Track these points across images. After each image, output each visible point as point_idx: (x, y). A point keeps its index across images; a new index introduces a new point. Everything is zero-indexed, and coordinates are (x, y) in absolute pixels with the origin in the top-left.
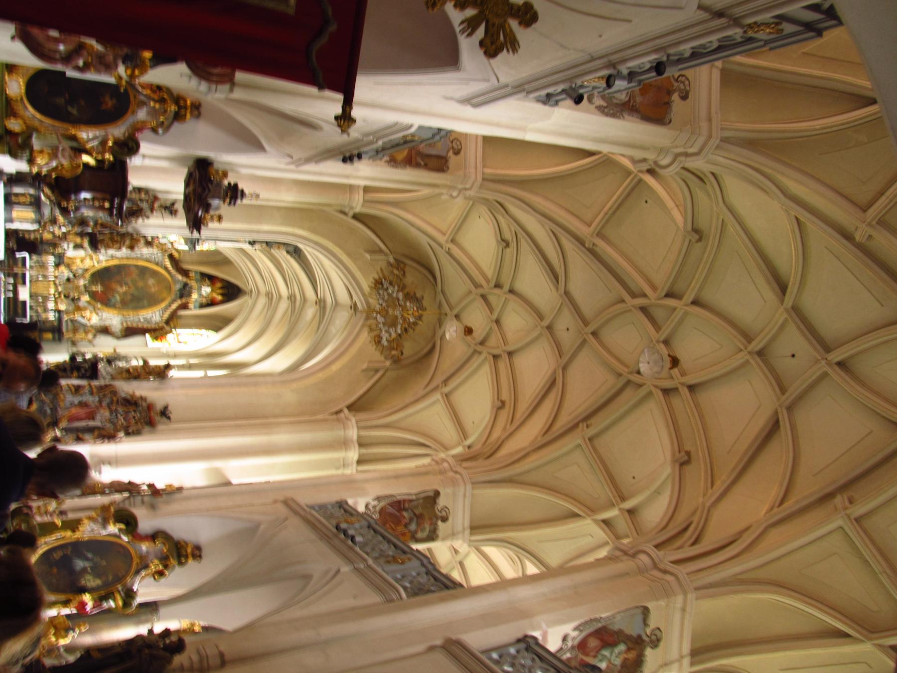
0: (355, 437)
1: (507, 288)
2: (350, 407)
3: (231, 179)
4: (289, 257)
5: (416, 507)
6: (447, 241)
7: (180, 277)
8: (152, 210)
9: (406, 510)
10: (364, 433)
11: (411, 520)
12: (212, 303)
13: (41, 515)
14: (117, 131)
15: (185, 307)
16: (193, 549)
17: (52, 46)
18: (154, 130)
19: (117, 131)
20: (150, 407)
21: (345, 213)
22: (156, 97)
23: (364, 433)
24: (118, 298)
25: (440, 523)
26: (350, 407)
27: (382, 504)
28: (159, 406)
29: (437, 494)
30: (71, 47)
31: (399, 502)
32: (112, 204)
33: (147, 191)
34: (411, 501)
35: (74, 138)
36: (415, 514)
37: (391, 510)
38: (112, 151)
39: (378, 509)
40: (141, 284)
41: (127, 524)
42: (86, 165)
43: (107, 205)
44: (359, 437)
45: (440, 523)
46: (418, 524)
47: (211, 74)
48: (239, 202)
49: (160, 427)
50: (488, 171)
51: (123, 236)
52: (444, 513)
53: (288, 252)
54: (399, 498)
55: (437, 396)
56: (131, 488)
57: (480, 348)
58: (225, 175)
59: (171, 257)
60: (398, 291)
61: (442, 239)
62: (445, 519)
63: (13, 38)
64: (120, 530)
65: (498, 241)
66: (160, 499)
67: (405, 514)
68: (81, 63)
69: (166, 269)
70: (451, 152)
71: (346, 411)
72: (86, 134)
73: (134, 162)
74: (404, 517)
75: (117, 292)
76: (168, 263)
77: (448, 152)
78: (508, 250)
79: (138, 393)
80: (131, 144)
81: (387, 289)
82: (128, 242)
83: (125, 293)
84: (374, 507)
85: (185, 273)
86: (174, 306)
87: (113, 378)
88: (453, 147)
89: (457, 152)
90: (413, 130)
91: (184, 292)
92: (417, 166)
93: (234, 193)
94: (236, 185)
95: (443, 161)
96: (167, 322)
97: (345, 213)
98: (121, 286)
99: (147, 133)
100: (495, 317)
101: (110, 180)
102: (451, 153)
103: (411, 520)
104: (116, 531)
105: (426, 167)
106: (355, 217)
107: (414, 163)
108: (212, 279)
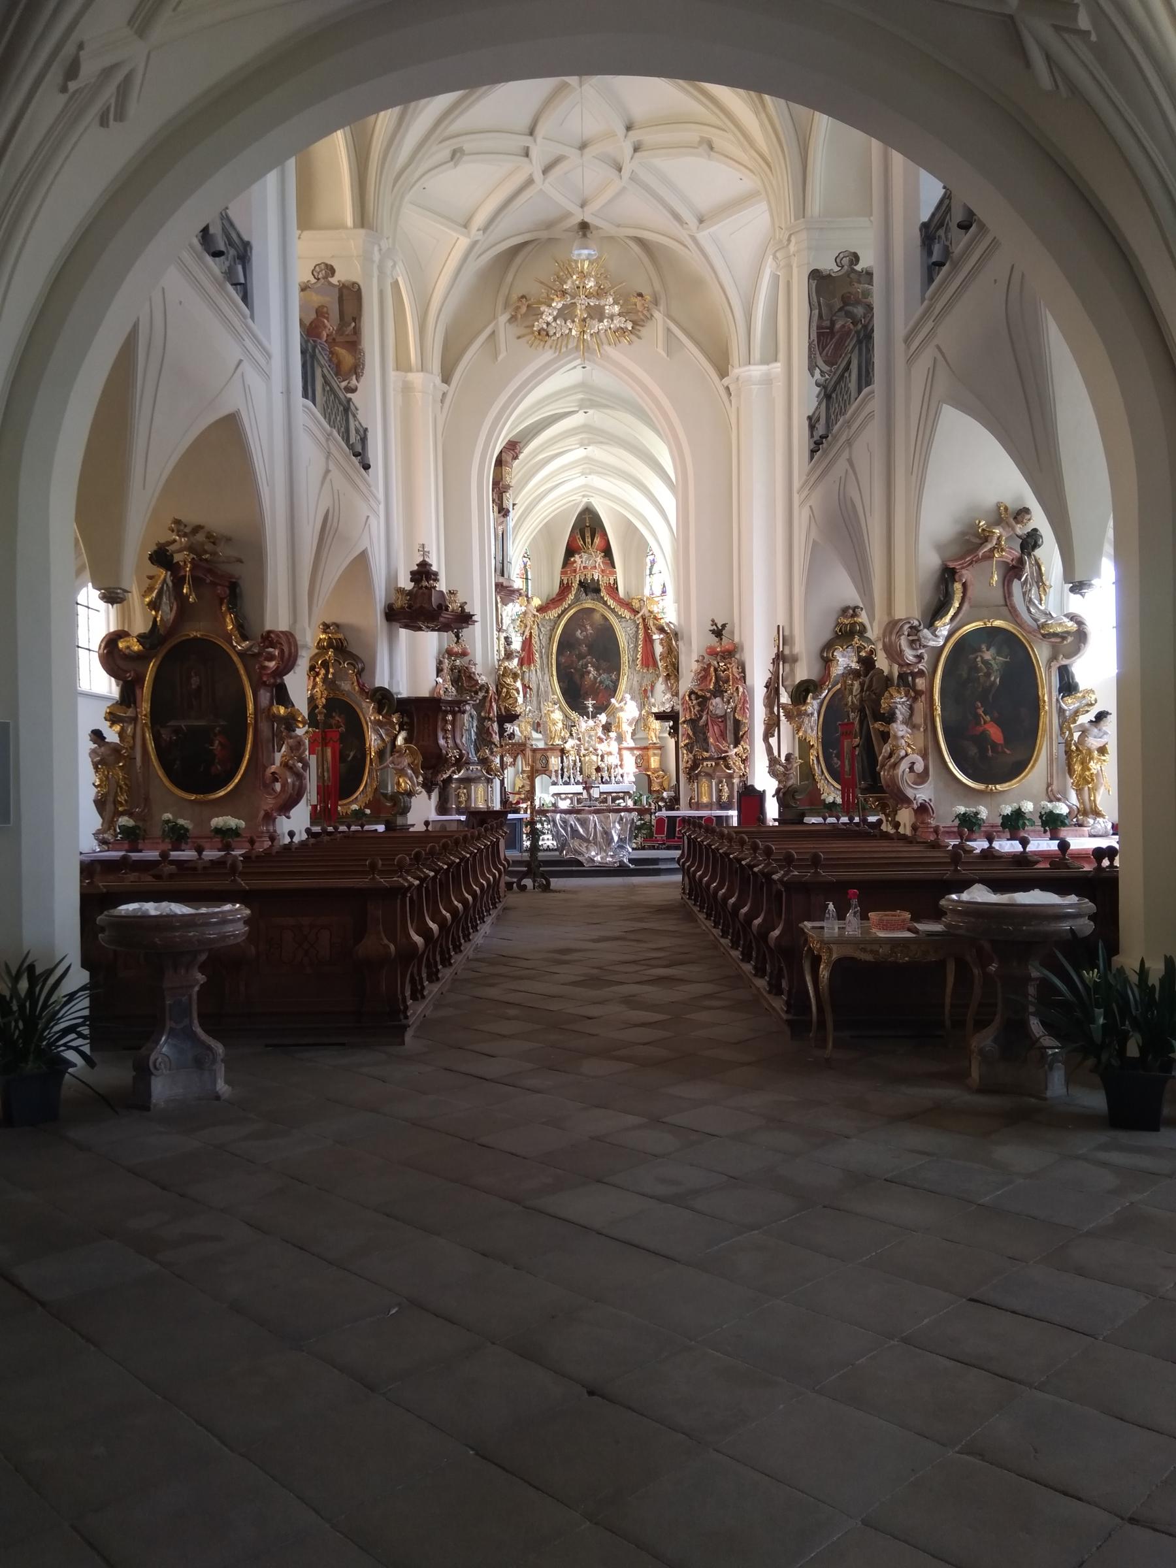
0: (764, 368)
1: (526, 141)
2: (723, 373)
3: (405, 583)
4: (521, 457)
5: (830, 307)
6: (468, 235)
7: (571, 597)
8: (464, 654)
9: (833, 323)
10: (757, 353)
11: (849, 314)
12: (607, 552)
13: (788, 779)
14: (369, 712)
15: (613, 589)
16: (846, 617)
17: (290, 789)
18: (359, 673)
19: (369, 712)
20: (712, 653)
21: (444, 394)
22: (323, 671)
23: (757, 353)
24: (604, 676)
25: (858, 268)
26: (723, 373)
27: (820, 362)
28: (713, 640)
29: (815, 275)
30: (288, 774)
31: (819, 335)
32: (446, 713)
33: (440, 663)
34: (820, 316)
35: (381, 754)
36: (841, 309)
37: (830, 348)
38: (388, 716)
39: (826, 368)
40: (584, 648)
41: (807, 692)
42: (406, 740)
43: (450, 717)
44: (764, 361)
45: (858, 268)
46: (858, 302)
47: (290, 653)
48: (434, 568)
50: (349, 222)
51: (500, 685)
52: (846, 261)
53: (515, 458)
54: (814, 336)
55: (703, 236)
56: (772, 689)
57: (626, 173)
58: (401, 591)
59: (541, 609)
60: (550, 306)
61: (464, 242)
62: (855, 258)
63: (288, 818)
64: (814, 698)
65: (456, 165)
66: (787, 652)
67: (838, 326)
68: (300, 765)
69: (559, 616)
70: (331, 280)
71: (726, 381)
72: (373, 741)
73: (403, 690)
74: (843, 326)
75: (595, 678)
76: (553, 614)
77: (330, 284)
78: (467, 147)
79: (695, 666)
80: (378, 696)
81: (548, 324)
82: (509, 680)
83: (597, 669)
84: (822, 373)
85: (565, 589)
86: (611, 602)
87: (677, 694)
88: (325, 278)
89: (331, 270)
90: (309, 403)
91: (590, 588)
92: (357, 332)
93: (423, 573)
94: (412, 573)
95: (345, 291)
96: (635, 612)
97: (444, 394)
98: (589, 672)
99: (365, 678)
100: (573, 153)
101: (422, 714)
102: (334, 281)
103: (849, 314)
104: (816, 703)
105: (357, 318)
106: (446, 379)
107: (354, 338)
108: (571, 551)
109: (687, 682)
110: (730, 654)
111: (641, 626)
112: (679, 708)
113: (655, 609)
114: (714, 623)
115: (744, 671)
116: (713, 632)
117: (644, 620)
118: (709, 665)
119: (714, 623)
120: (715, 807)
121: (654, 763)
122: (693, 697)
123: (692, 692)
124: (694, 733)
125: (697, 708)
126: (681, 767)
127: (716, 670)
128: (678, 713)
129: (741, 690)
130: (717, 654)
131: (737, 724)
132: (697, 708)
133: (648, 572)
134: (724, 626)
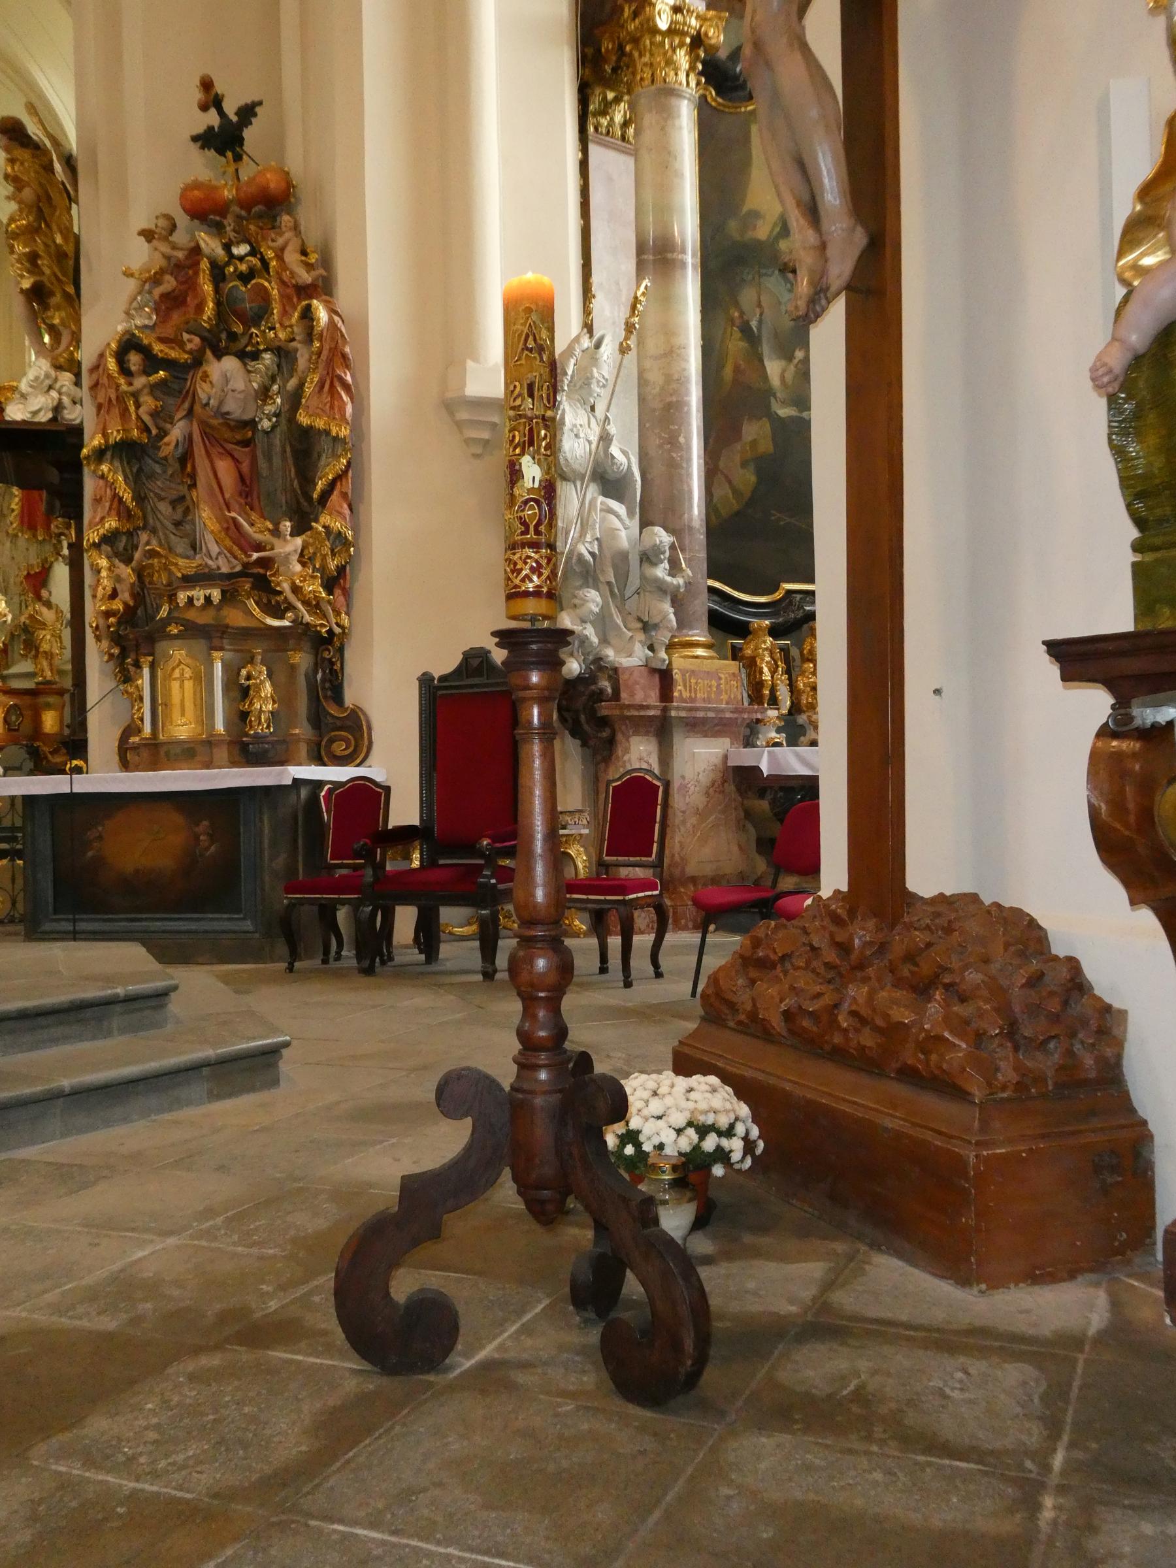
20: (204, 210)
28: (202, 167)
49: (295, 164)
79: (141, 255)
109: (108, 313)
110: (272, 204)
112: (81, 414)
114: (212, 100)
115: (327, 261)
116: (205, 140)
118: (196, 251)
119: (212, 100)
120: (222, 753)
121: (50, 721)
122: (134, 359)
123: (128, 345)
124: (140, 498)
125: (149, 403)
126: (92, 610)
127: (218, 274)
128: (77, 432)
129: (322, 315)
130: (222, 209)
131: (305, 447)
132: (149, 403)
134: (248, 112)
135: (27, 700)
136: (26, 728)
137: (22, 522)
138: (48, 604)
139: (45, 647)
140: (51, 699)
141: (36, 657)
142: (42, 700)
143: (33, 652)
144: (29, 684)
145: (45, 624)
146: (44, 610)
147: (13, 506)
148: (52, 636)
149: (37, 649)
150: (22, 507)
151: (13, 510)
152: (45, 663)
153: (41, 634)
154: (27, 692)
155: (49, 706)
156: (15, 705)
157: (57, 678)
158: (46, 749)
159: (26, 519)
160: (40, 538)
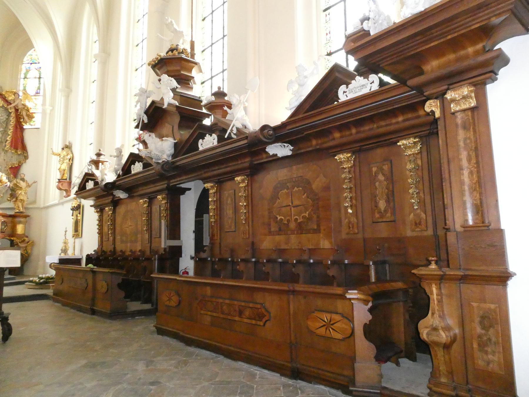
111: (13, 115)
113: (29, 104)
117: (17, 110)
121: (20, 229)
133: (23, 76)
135: (10, 219)
136: (8, 230)
137: (11, 146)
138: (23, 180)
139: (21, 197)
140: (22, 220)
141: (15, 201)
142: (17, 219)
143: (14, 199)
144: (12, 213)
145: (21, 188)
146: (21, 182)
147: (8, 139)
148: (25, 193)
149: (17, 199)
150: (12, 139)
151: (7, 140)
152: (20, 204)
153: (20, 192)
154: (11, 216)
155: (20, 222)
156: (4, 221)
157: (24, 211)
158: (18, 241)
159: (13, 144)
160: (19, 153)
